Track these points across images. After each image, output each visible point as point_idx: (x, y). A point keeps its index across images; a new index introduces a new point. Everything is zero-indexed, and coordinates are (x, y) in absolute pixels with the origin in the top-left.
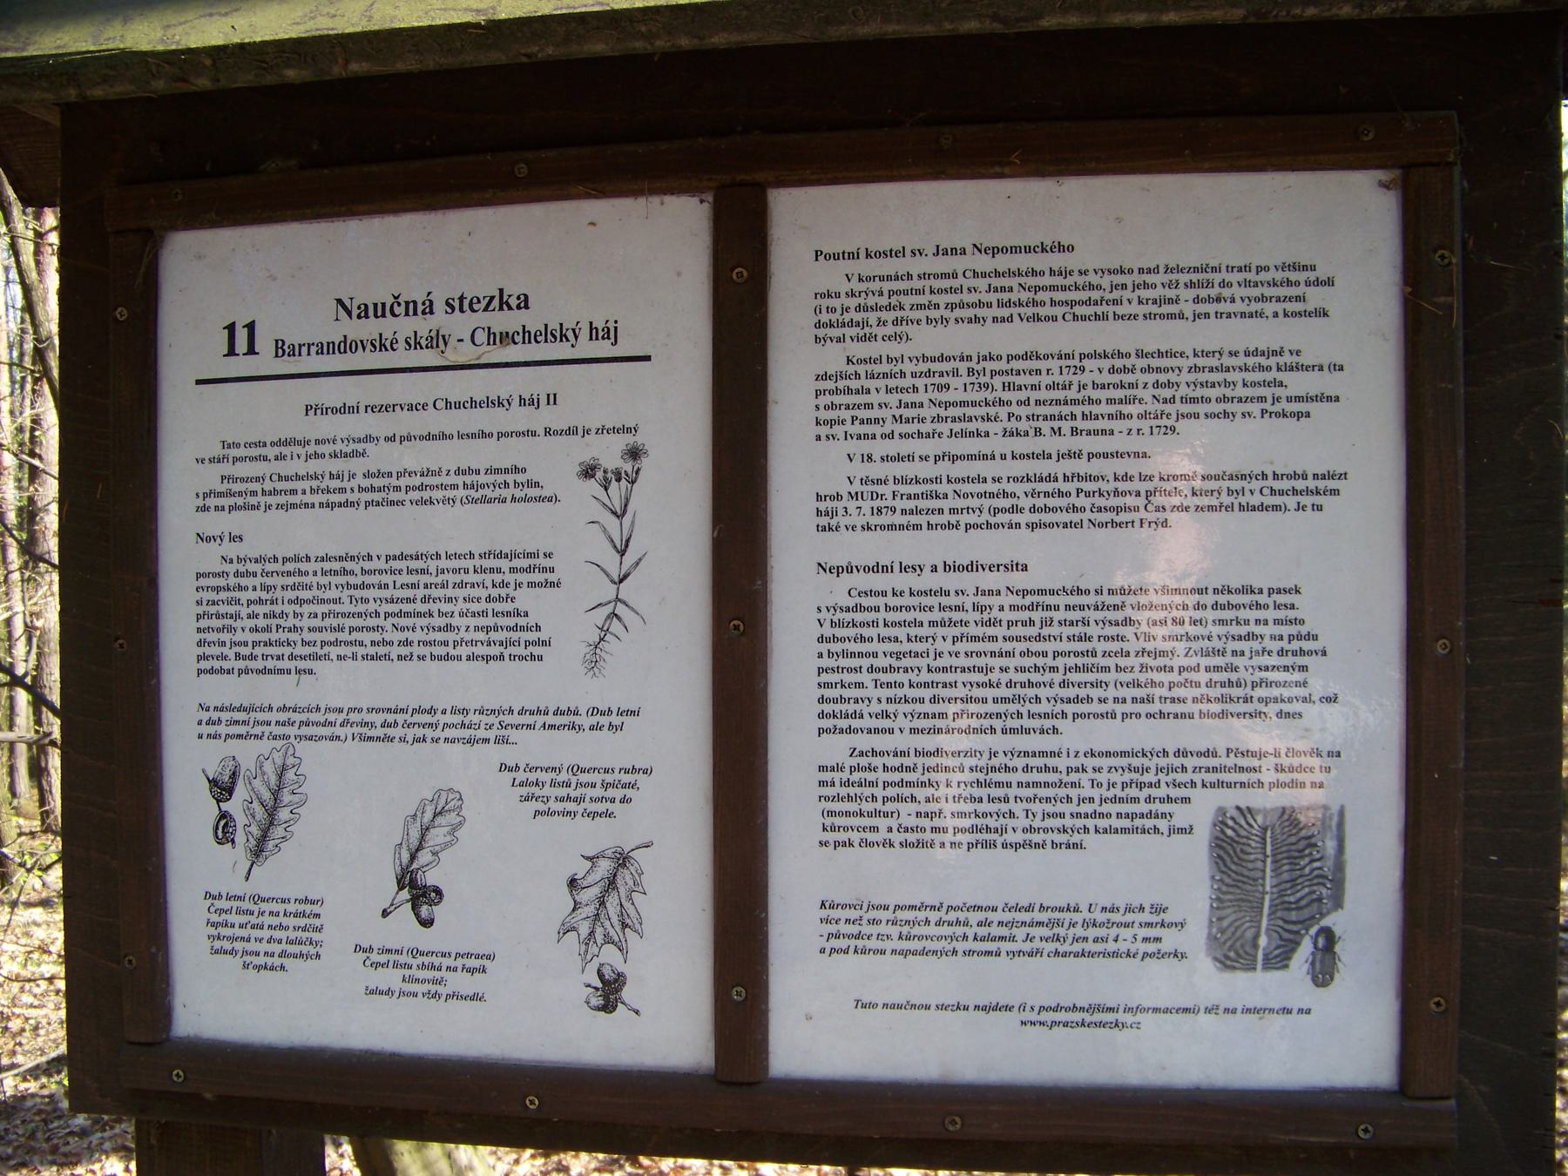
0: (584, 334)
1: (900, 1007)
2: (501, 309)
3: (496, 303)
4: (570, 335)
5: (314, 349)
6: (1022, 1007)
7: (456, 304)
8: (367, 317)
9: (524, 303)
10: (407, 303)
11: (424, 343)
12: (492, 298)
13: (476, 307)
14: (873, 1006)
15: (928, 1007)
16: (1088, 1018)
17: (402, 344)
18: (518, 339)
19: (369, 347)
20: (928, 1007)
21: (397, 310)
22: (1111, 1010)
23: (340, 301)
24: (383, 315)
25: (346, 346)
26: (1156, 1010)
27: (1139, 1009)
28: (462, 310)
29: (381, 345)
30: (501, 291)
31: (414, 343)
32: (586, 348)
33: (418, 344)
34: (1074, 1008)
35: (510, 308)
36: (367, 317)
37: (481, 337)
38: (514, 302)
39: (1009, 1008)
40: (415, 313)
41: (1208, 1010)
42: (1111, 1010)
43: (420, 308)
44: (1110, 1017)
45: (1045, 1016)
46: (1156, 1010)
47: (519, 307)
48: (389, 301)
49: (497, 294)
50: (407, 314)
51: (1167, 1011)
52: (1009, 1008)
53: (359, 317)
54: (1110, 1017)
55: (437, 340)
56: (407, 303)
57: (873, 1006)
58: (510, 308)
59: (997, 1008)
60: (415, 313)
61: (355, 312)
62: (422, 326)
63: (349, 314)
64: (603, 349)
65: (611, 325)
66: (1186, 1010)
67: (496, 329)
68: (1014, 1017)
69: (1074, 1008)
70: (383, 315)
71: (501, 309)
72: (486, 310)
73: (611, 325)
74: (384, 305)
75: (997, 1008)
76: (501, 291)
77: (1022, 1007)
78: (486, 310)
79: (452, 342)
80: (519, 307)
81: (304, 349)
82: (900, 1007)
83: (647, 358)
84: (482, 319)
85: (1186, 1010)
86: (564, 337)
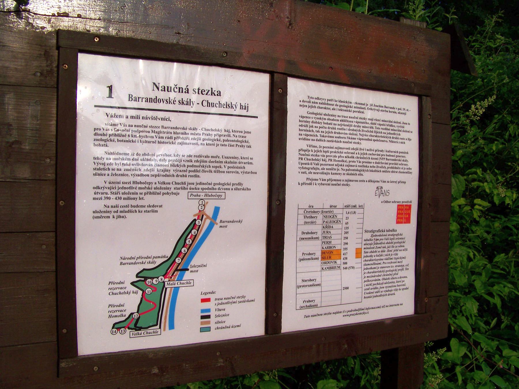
0: (238, 107)
1: (315, 316)
2: (212, 95)
3: (210, 93)
4: (234, 106)
5: (144, 100)
6: (344, 312)
7: (197, 91)
8: (165, 91)
9: (219, 94)
10: (180, 88)
11: (185, 103)
12: (209, 91)
13: (203, 93)
14: (309, 316)
15: (322, 315)
16: (357, 312)
17: (177, 102)
18: (217, 106)
19: (165, 102)
20: (322, 315)
21: (176, 90)
22: (363, 309)
23: (154, 83)
24: (171, 91)
25: (156, 100)
26: (372, 308)
27: (369, 309)
28: (198, 93)
29: (168, 101)
30: (212, 88)
31: (182, 102)
32: (238, 111)
33: (183, 103)
34: (355, 310)
35: (215, 95)
36: (165, 91)
37: (205, 103)
38: (216, 93)
39: (341, 312)
40: (182, 92)
41: (383, 307)
42: (363, 309)
43: (184, 91)
44: (362, 311)
45: (349, 313)
46: (372, 308)
47: (218, 95)
48: (173, 86)
49: (210, 89)
50: (179, 92)
51: (374, 308)
52: (341, 312)
53: (162, 90)
54: (362, 311)
55: (189, 103)
56: (180, 88)
57: (309, 316)
58: (215, 95)
59: (338, 313)
60: (182, 92)
61: (160, 88)
62: (185, 97)
63: (158, 89)
64: (244, 112)
65: (246, 105)
66: (378, 307)
67: (210, 102)
68: (342, 314)
69: (355, 310)
70: (171, 91)
71: (212, 95)
72: (207, 94)
73: (246, 105)
74: (171, 87)
75: (338, 313)
76: (212, 88)
77: (344, 312)
78: (207, 94)
79: (195, 104)
80: (218, 95)
81: (140, 100)
82: (315, 316)
83: (257, 117)
84: (205, 97)
85: (378, 307)
86: (232, 107)
